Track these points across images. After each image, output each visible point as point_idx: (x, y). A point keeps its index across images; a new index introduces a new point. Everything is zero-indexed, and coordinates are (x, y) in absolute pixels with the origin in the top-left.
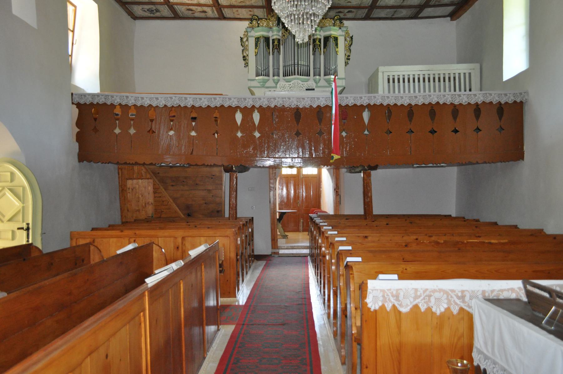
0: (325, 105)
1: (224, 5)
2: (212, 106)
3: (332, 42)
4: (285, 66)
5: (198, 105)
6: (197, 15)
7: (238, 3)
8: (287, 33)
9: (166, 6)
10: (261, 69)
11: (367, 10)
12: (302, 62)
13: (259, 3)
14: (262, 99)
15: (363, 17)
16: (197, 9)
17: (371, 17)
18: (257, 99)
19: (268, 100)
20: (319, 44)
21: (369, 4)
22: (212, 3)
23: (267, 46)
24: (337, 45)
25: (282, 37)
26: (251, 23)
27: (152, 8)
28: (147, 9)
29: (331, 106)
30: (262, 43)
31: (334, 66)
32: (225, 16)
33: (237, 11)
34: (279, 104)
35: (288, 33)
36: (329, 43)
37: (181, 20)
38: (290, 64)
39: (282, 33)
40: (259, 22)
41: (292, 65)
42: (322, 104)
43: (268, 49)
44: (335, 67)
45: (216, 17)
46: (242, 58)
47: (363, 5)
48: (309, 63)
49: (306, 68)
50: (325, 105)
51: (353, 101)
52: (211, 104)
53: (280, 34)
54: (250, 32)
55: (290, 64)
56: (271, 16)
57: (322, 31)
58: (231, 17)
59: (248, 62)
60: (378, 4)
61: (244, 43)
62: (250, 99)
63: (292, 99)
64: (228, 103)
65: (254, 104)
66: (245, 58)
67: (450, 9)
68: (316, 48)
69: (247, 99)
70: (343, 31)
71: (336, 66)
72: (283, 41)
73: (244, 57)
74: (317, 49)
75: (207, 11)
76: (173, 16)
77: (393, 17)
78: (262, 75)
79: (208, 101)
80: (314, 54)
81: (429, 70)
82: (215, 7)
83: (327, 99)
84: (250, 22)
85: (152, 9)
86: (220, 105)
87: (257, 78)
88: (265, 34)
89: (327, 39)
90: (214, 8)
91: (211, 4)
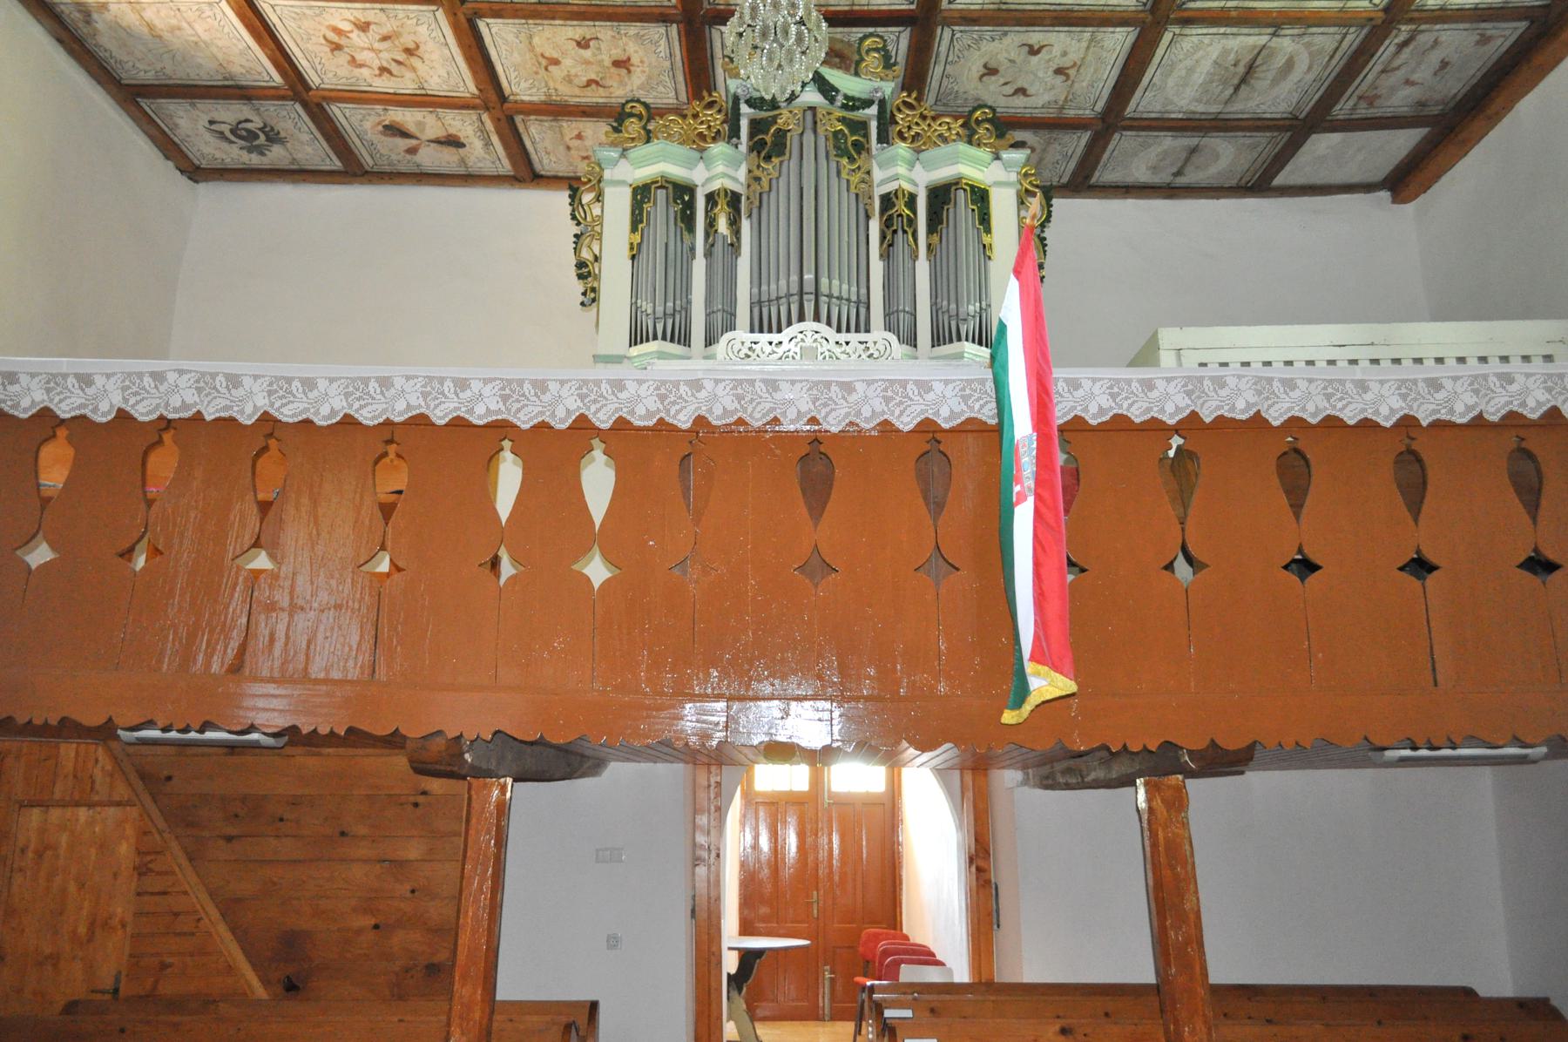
0: (959, 421)
2: (368, 416)
3: (962, 208)
4: (760, 302)
5: (294, 415)
6: (431, 158)
7: (577, 91)
9: (298, 107)
10: (654, 312)
11: (1086, 137)
12: (836, 282)
13: (661, 89)
15: (1065, 180)
16: (420, 125)
17: (1093, 180)
18: (603, 386)
19: (663, 391)
20: (908, 215)
21: (1099, 107)
22: (476, 92)
23: (682, 221)
24: (985, 220)
25: (749, 186)
27: (247, 121)
28: (229, 127)
30: (661, 209)
31: (978, 304)
32: (537, 167)
33: (579, 137)
34: (718, 411)
36: (951, 210)
37: (370, 182)
38: (782, 294)
39: (750, 171)
40: (651, 127)
41: (789, 295)
42: (945, 412)
43: (685, 233)
44: (981, 308)
45: (502, 172)
46: (573, 272)
48: (863, 291)
49: (854, 312)
50: (963, 418)
51: (1105, 402)
52: (362, 407)
54: (615, 163)
55: (783, 292)
57: (918, 166)
58: (560, 174)
59: (596, 285)
60: (1093, 180)
61: (586, 208)
62: (567, 386)
64: (452, 406)
66: (584, 270)
67: (1403, 142)
68: (895, 232)
70: (1007, 166)
71: (984, 303)
72: (752, 199)
73: (581, 265)
75: (462, 140)
76: (337, 164)
77: (1182, 181)
78: (655, 338)
79: (347, 395)
80: (886, 255)
81: (1372, 344)
82: (487, 109)
83: (968, 392)
84: (615, 124)
85: (249, 126)
86: (410, 414)
87: (635, 351)
88: (677, 172)
89: (941, 196)
90: (485, 117)
91: (474, 97)
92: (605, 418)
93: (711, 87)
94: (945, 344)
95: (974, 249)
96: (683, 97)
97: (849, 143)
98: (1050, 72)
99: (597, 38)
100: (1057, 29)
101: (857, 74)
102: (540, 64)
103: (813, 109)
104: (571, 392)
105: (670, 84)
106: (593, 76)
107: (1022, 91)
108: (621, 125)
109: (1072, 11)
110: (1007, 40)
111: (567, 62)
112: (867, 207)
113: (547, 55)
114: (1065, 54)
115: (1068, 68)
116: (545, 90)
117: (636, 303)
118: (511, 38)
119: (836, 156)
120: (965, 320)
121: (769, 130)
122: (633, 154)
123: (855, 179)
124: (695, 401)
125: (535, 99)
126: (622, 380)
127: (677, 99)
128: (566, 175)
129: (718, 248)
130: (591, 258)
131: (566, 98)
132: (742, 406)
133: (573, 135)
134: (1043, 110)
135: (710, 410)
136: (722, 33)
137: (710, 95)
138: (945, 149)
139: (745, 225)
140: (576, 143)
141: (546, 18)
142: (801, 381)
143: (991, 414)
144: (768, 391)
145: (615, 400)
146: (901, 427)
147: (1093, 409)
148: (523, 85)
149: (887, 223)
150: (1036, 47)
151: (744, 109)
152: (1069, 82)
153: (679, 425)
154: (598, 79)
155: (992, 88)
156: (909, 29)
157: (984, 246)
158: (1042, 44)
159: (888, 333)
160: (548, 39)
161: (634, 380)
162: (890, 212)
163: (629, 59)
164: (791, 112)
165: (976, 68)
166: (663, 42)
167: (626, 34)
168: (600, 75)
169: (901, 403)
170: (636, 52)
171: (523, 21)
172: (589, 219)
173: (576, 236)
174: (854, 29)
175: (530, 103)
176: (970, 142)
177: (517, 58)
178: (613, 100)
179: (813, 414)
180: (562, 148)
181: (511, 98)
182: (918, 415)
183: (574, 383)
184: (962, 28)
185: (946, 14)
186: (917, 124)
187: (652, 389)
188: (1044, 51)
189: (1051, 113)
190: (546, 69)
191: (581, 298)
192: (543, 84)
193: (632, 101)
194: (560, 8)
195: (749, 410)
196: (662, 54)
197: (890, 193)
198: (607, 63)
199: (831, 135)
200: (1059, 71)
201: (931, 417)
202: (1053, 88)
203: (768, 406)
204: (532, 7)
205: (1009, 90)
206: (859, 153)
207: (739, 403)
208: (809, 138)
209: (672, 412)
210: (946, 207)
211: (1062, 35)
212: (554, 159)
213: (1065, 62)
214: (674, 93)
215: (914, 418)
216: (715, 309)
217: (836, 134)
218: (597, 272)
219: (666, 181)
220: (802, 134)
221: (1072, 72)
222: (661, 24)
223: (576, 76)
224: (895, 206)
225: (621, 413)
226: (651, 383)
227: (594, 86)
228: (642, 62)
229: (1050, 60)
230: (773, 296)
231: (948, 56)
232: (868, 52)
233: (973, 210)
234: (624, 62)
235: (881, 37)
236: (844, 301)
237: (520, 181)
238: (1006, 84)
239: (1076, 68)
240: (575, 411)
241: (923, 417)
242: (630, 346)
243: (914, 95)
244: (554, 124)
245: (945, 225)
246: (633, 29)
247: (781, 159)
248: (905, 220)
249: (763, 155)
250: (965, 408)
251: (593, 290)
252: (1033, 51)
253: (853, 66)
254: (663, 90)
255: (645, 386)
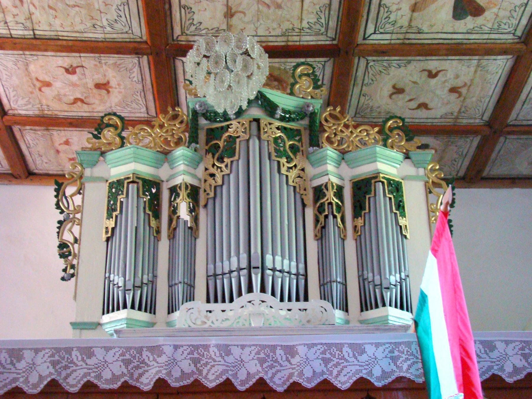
0: (390, 380)
1: (20, 115)
7: (66, 107)
8: (223, 166)
10: (125, 286)
11: (476, 140)
12: (278, 258)
13: (134, 105)
14: (97, 351)
15: (461, 174)
17: (485, 174)
18: (75, 353)
19: (128, 357)
20: (337, 203)
21: (486, 117)
24: (400, 206)
25: (205, 181)
26: (96, 137)
29: (421, 380)
32: (32, 167)
33: (67, 143)
34: (177, 373)
35: (226, 166)
36: (372, 200)
39: (206, 169)
40: (124, 134)
41: (240, 269)
42: (377, 372)
44: (401, 278)
46: (56, 251)
47: (465, 122)
48: (302, 266)
50: (393, 377)
53: (200, 172)
55: (234, 267)
56: (168, 116)
57: (343, 165)
58: (51, 172)
59: (75, 262)
62: (41, 354)
63: (236, 352)
65: (59, 374)
68: (326, 217)
69: (28, 355)
71: (403, 275)
72: (208, 191)
73: (63, 246)
74: (331, 217)
78: (125, 307)
83: (396, 353)
84: (96, 133)
87: (106, 318)
92: (74, 382)
93: (176, 103)
94: (372, 308)
95: (392, 231)
96: (153, 112)
97: (287, 147)
98: (446, 89)
99: (83, 67)
100: (450, 58)
101: (292, 94)
102: (34, 85)
103: (257, 121)
104: (45, 359)
105: (142, 102)
106: (79, 96)
107: (424, 106)
108: (100, 133)
109: (462, 44)
110: (411, 67)
111: (57, 84)
112: (303, 197)
113: (41, 78)
114: (457, 77)
115: (459, 88)
116: (39, 106)
117: (109, 277)
118: (10, 65)
119: (276, 156)
120: (388, 288)
121: (221, 137)
122: (110, 156)
123: (293, 174)
124: (156, 364)
125: (30, 113)
126: (91, 348)
127: (148, 113)
128: (55, 173)
129: (180, 232)
130: (72, 240)
131: (56, 112)
132: (198, 369)
133: (62, 142)
134: (442, 120)
135: (169, 374)
136: (183, 63)
137: (174, 110)
138: (364, 152)
139: (202, 214)
140: (62, 148)
141: (39, 50)
142: (250, 346)
143: (418, 373)
144: (221, 355)
145: (84, 366)
146: (339, 386)
147: (509, 368)
148: (21, 102)
149: (320, 210)
150: (434, 72)
151: (203, 122)
152: (462, 99)
153: (142, 387)
154: (83, 98)
155: (400, 103)
156: (332, 59)
157: (401, 227)
158: (439, 69)
159: (323, 301)
160: (42, 66)
161: (101, 348)
162: (322, 201)
163: (108, 82)
164: (239, 123)
165: (387, 90)
166: (136, 70)
167: (105, 63)
168: (85, 95)
169: (338, 364)
170: (115, 77)
171: (21, 52)
172: (71, 208)
173: (60, 222)
174: (289, 60)
175: (26, 116)
176: (385, 145)
177: (15, 80)
178: (95, 114)
179: (261, 375)
180: (52, 152)
181: (10, 112)
182: (354, 375)
183: (47, 351)
184: (374, 58)
185: (362, 48)
186: (342, 131)
187: (117, 354)
188: (440, 75)
189: (449, 121)
190: (40, 90)
191: (63, 274)
192: (37, 101)
193: (110, 114)
194: (52, 43)
195: (205, 372)
196: (135, 79)
197: (322, 185)
198: (91, 85)
199: (272, 140)
200: (453, 90)
201: (365, 376)
202: (448, 103)
203: (221, 368)
204: (29, 42)
205: (413, 104)
206: (295, 154)
207: (195, 366)
208: (254, 144)
209: (136, 376)
210: (367, 197)
211: (455, 63)
212: (45, 161)
213: (459, 83)
214: (145, 109)
215: (350, 378)
216: (177, 282)
217: (276, 139)
218: (76, 252)
219: (139, 178)
220: (248, 141)
221: (464, 91)
222: (133, 56)
223: (65, 95)
224: (325, 196)
225: (89, 378)
226: (117, 349)
227: (79, 103)
228: (119, 85)
229: (445, 81)
230: (226, 270)
231: (364, 80)
232: (300, 77)
233: (390, 199)
234: (105, 85)
235: (311, 65)
236: (286, 274)
237: (16, 178)
238: (411, 100)
239: (466, 88)
240: (47, 376)
241: (358, 376)
242: (103, 314)
243: (338, 109)
244: (45, 132)
245: (367, 211)
246: (112, 59)
247: (231, 159)
248: (334, 207)
249: (216, 156)
250: (395, 368)
251: (73, 267)
252: (432, 75)
253: (289, 87)
254: (136, 106)
255: (111, 352)
